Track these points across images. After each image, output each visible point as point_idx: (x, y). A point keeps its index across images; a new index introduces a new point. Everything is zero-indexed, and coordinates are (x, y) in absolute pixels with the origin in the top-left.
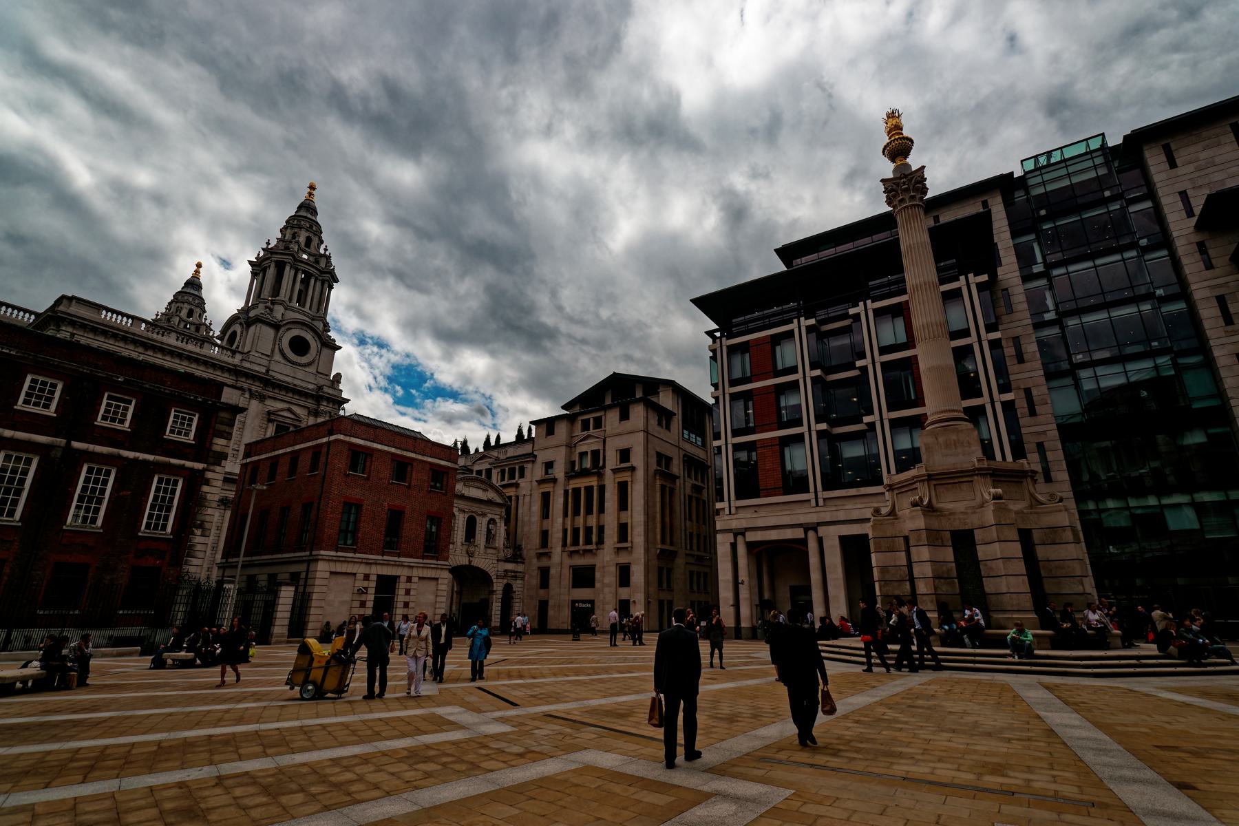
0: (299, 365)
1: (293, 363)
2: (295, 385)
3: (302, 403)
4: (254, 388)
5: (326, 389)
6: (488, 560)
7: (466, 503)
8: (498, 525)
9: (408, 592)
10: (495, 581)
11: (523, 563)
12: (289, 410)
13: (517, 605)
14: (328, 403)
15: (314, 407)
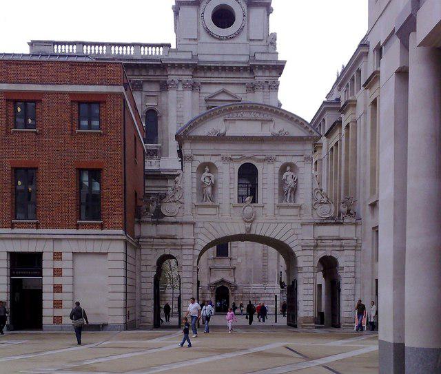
0: (227, 38)
1: (220, 38)
2: (224, 63)
3: (236, 81)
4: (184, 79)
5: (258, 57)
6: (281, 226)
7: (233, 147)
8: (301, 170)
9: (58, 272)
10: (297, 254)
11: (356, 224)
12: (224, 92)
13: (349, 287)
14: (263, 72)
15: (249, 81)
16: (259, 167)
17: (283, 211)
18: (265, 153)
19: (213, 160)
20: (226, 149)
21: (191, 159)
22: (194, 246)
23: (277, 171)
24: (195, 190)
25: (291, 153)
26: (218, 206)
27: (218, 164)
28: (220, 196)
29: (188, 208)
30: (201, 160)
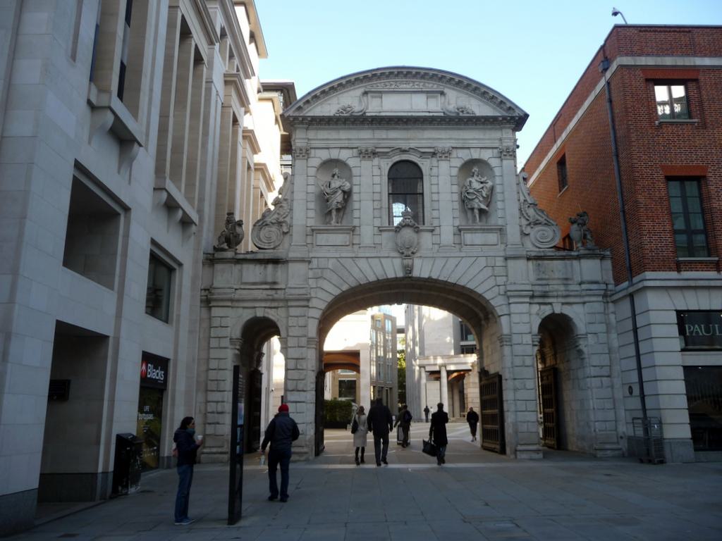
8: (497, 171)
16: (425, 165)
17: (468, 238)
18: (435, 144)
19: (344, 155)
20: (366, 137)
21: (306, 153)
22: (308, 300)
23: (455, 172)
24: (312, 205)
25: (478, 143)
26: (353, 231)
27: (351, 163)
28: (356, 214)
29: (297, 236)
30: (324, 155)
